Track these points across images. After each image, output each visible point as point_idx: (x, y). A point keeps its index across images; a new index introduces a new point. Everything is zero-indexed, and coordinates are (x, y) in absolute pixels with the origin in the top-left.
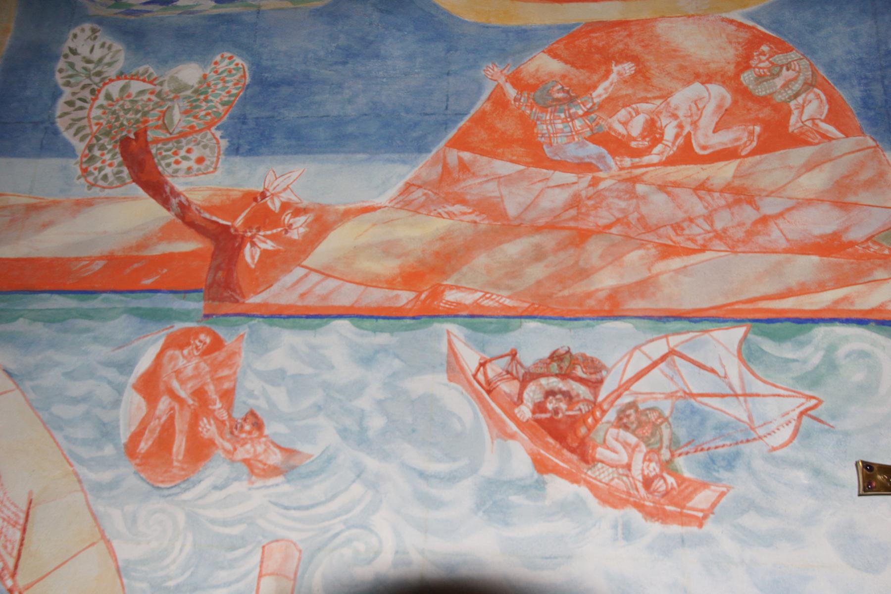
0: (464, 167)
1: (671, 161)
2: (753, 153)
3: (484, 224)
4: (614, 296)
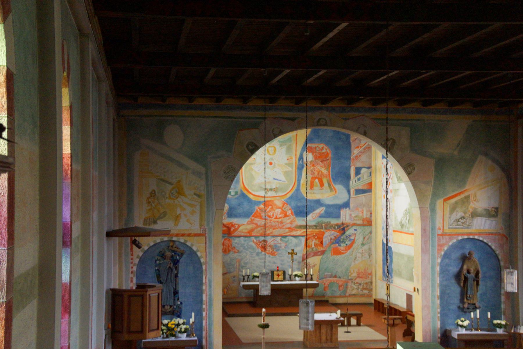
0: (254, 219)
1: (275, 218)
2: (284, 217)
3: (256, 226)
4: (269, 234)
